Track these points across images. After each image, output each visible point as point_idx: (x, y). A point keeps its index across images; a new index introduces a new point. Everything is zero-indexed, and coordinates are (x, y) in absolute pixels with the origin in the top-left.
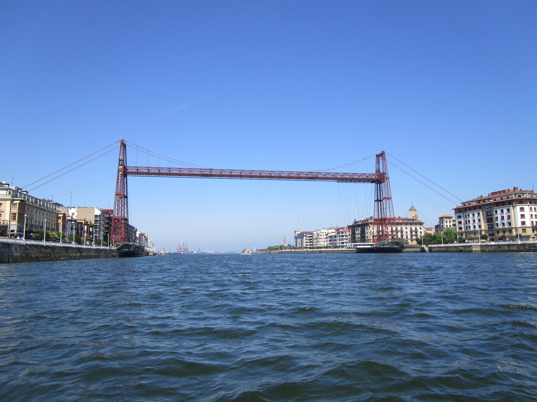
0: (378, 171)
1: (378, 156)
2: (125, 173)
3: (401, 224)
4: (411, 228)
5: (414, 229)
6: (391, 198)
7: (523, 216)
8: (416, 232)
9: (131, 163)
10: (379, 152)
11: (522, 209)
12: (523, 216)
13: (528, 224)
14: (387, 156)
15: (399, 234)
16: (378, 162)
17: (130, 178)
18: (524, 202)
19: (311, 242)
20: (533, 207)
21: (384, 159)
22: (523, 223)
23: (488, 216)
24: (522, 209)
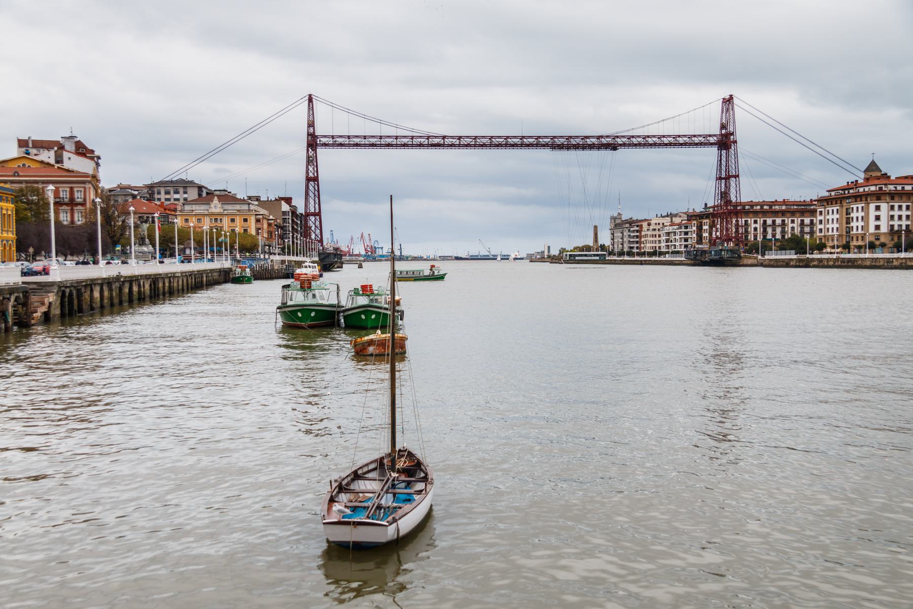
2: (313, 142)
3: (783, 213)
4: (802, 221)
5: (807, 221)
6: (738, 176)
7: (878, 218)
8: (812, 229)
11: (878, 208)
12: (878, 218)
13: (884, 229)
15: (779, 230)
17: (320, 151)
18: (882, 198)
19: (637, 242)
20: (896, 205)
24: (878, 208)
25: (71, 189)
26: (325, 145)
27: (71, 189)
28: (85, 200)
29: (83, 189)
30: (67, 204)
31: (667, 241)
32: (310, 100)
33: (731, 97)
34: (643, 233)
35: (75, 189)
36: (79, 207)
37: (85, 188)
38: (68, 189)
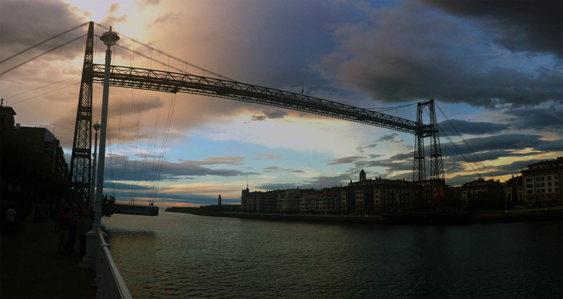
1: (420, 105)
16: (420, 112)
31: (306, 204)
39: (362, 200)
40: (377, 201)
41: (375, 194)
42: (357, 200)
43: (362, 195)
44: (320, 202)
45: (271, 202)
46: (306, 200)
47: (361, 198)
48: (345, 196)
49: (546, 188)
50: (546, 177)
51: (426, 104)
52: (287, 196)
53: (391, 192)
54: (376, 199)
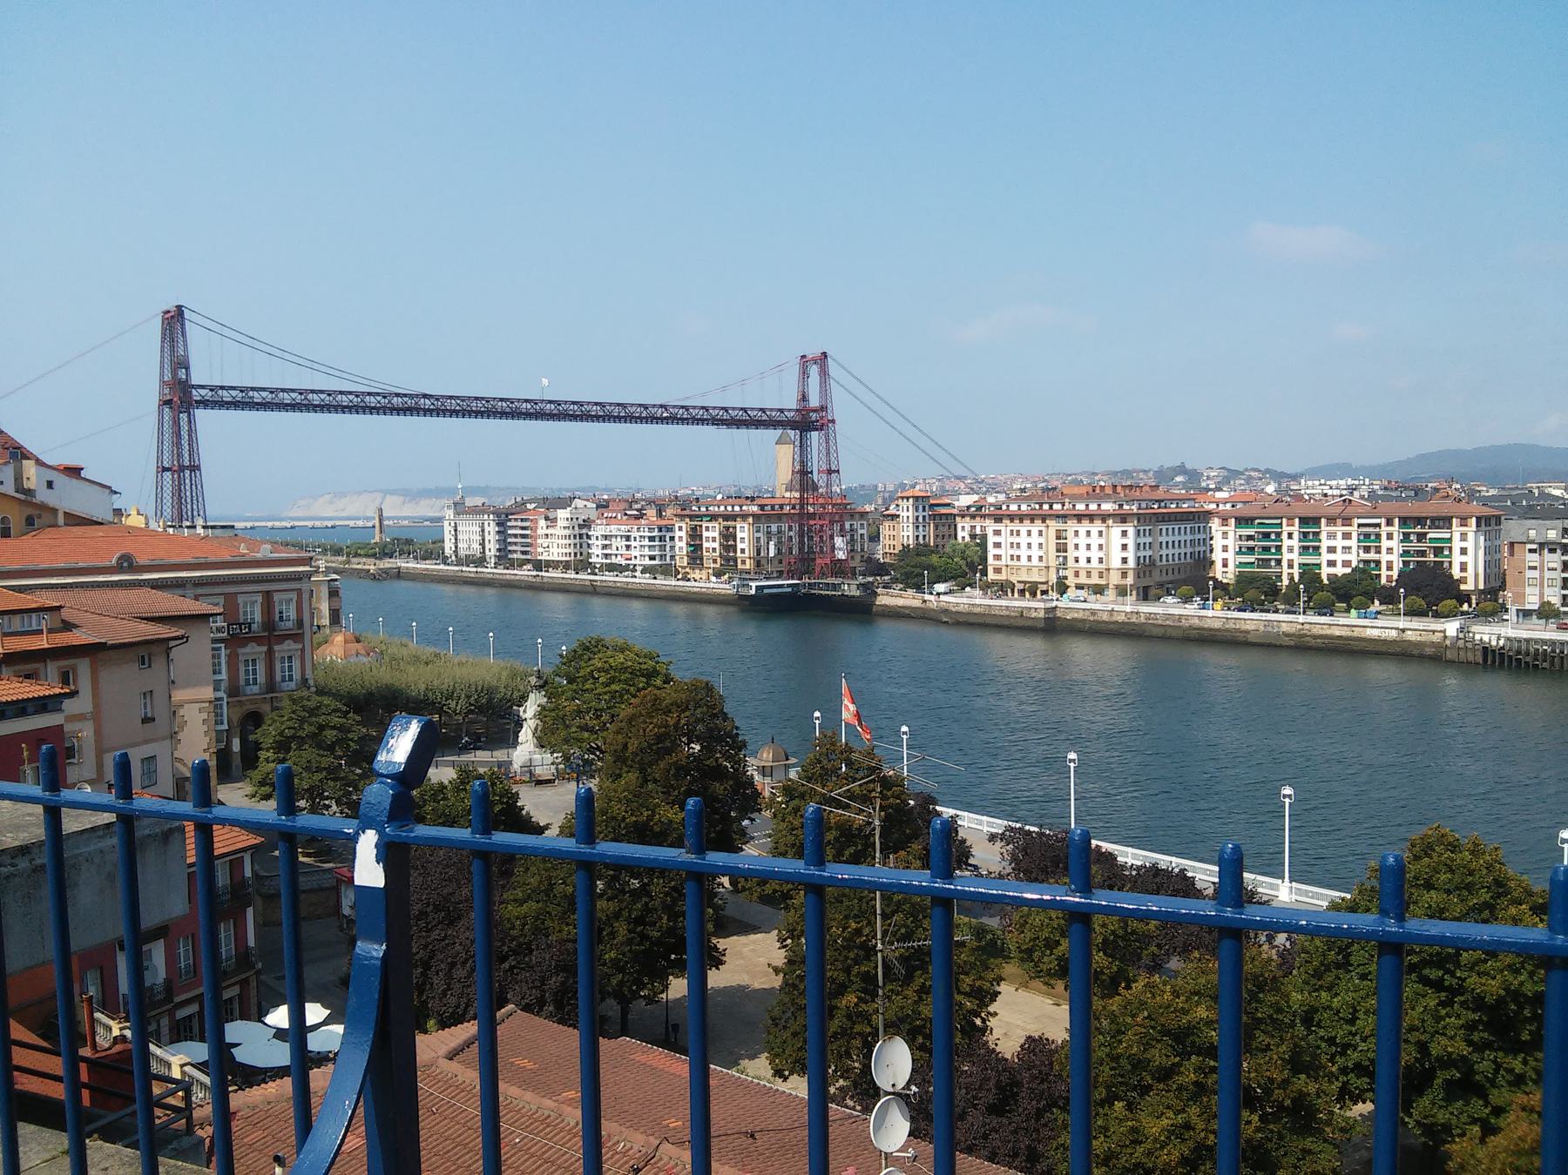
0: (804, 398)
2: (181, 398)
7: (1124, 547)
9: (201, 374)
10: (813, 351)
11: (1124, 533)
12: (1124, 547)
14: (833, 368)
16: (804, 374)
21: (824, 373)
22: (1125, 560)
23: (1058, 538)
24: (1124, 533)
25: (268, 595)
26: (205, 403)
27: (268, 595)
28: (300, 623)
29: (294, 596)
30: (258, 640)
31: (605, 547)
32: (174, 320)
33: (824, 354)
34: (540, 532)
35: (276, 597)
36: (289, 645)
37: (299, 591)
38: (260, 599)
39: (716, 545)
40: (743, 551)
41: (739, 535)
42: (705, 545)
43: (716, 534)
44: (633, 543)
45: (524, 536)
46: (606, 537)
47: (714, 540)
48: (683, 534)
49: (1024, 552)
50: (1024, 531)
51: (815, 361)
52: (561, 523)
53: (774, 528)
54: (740, 546)
